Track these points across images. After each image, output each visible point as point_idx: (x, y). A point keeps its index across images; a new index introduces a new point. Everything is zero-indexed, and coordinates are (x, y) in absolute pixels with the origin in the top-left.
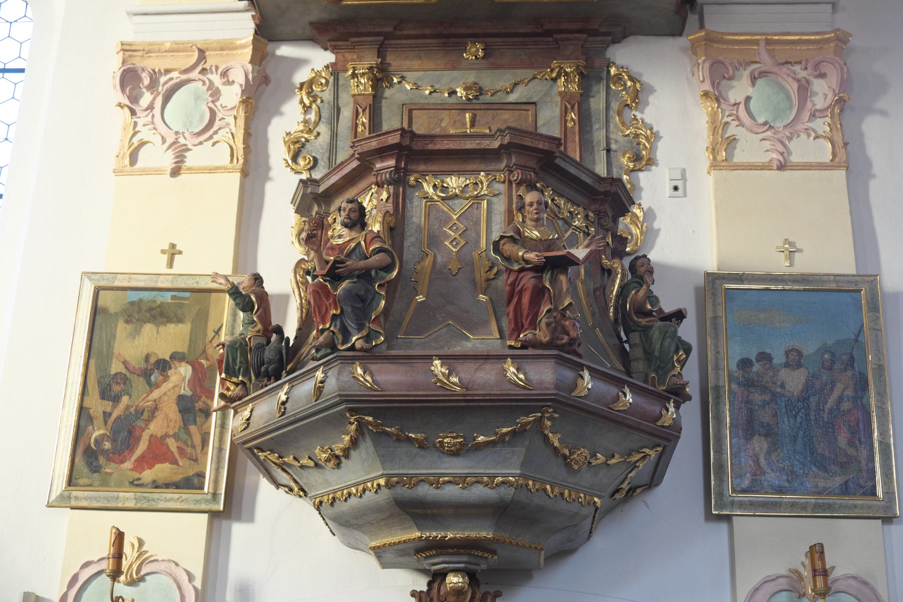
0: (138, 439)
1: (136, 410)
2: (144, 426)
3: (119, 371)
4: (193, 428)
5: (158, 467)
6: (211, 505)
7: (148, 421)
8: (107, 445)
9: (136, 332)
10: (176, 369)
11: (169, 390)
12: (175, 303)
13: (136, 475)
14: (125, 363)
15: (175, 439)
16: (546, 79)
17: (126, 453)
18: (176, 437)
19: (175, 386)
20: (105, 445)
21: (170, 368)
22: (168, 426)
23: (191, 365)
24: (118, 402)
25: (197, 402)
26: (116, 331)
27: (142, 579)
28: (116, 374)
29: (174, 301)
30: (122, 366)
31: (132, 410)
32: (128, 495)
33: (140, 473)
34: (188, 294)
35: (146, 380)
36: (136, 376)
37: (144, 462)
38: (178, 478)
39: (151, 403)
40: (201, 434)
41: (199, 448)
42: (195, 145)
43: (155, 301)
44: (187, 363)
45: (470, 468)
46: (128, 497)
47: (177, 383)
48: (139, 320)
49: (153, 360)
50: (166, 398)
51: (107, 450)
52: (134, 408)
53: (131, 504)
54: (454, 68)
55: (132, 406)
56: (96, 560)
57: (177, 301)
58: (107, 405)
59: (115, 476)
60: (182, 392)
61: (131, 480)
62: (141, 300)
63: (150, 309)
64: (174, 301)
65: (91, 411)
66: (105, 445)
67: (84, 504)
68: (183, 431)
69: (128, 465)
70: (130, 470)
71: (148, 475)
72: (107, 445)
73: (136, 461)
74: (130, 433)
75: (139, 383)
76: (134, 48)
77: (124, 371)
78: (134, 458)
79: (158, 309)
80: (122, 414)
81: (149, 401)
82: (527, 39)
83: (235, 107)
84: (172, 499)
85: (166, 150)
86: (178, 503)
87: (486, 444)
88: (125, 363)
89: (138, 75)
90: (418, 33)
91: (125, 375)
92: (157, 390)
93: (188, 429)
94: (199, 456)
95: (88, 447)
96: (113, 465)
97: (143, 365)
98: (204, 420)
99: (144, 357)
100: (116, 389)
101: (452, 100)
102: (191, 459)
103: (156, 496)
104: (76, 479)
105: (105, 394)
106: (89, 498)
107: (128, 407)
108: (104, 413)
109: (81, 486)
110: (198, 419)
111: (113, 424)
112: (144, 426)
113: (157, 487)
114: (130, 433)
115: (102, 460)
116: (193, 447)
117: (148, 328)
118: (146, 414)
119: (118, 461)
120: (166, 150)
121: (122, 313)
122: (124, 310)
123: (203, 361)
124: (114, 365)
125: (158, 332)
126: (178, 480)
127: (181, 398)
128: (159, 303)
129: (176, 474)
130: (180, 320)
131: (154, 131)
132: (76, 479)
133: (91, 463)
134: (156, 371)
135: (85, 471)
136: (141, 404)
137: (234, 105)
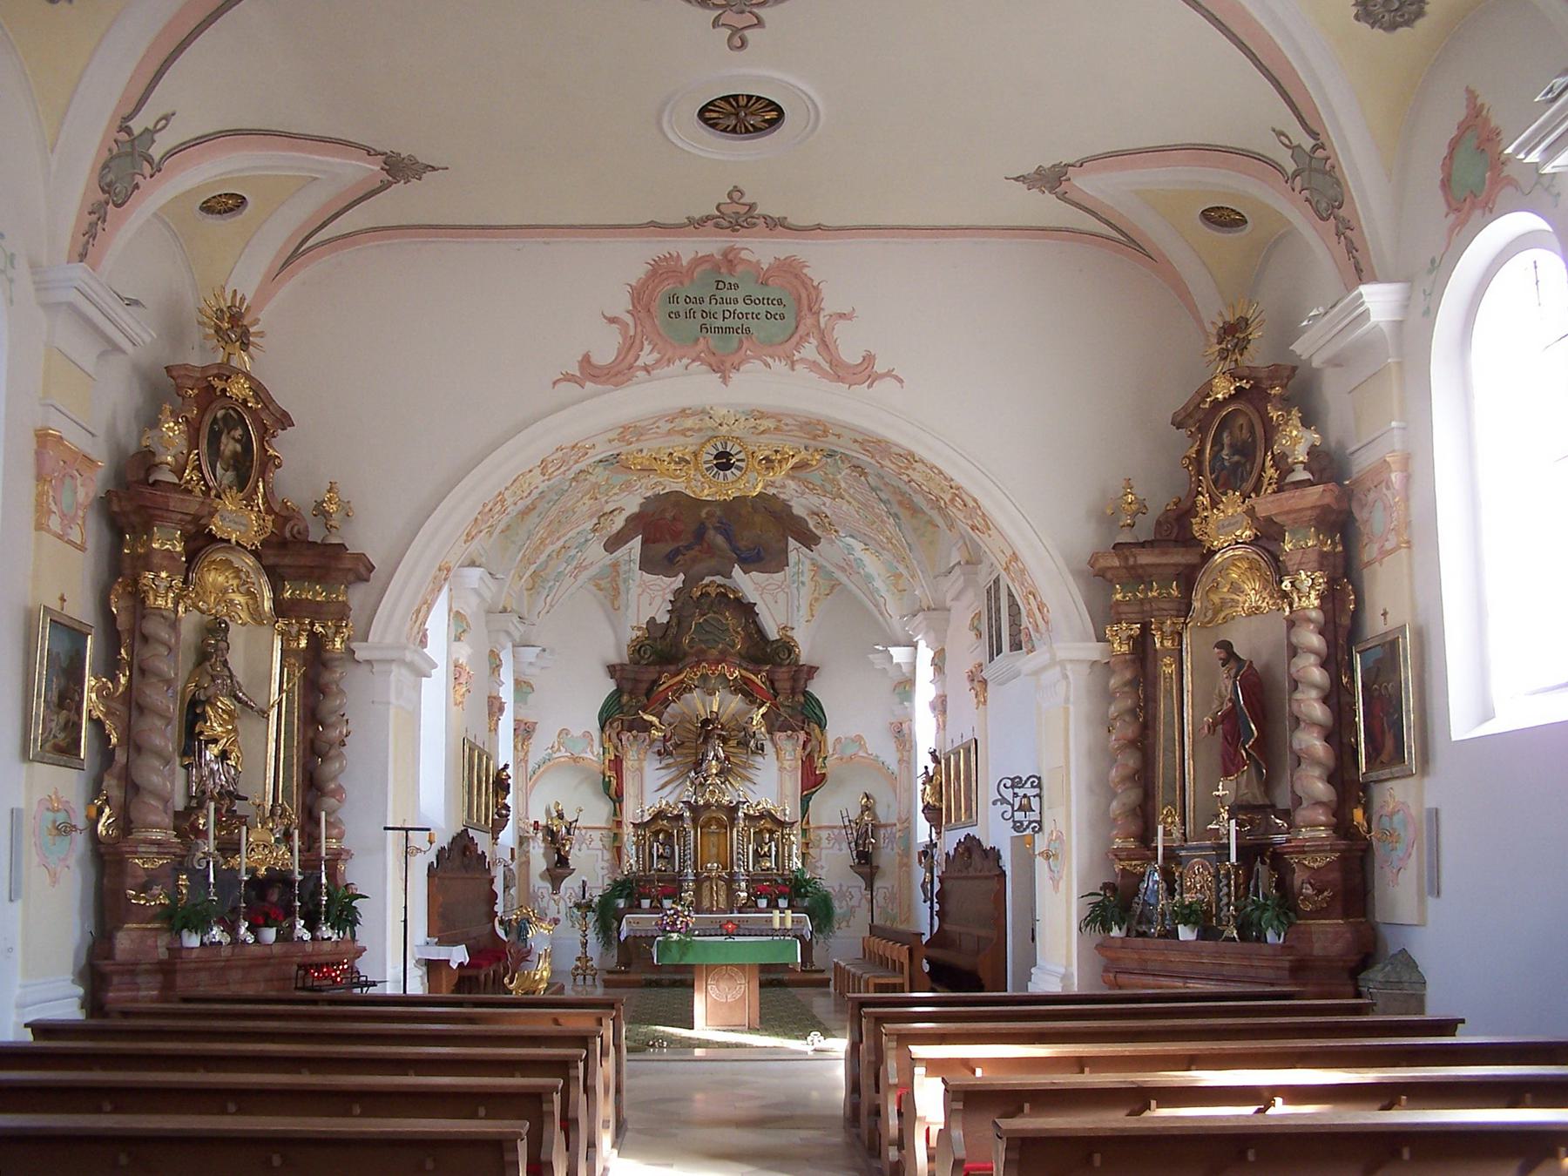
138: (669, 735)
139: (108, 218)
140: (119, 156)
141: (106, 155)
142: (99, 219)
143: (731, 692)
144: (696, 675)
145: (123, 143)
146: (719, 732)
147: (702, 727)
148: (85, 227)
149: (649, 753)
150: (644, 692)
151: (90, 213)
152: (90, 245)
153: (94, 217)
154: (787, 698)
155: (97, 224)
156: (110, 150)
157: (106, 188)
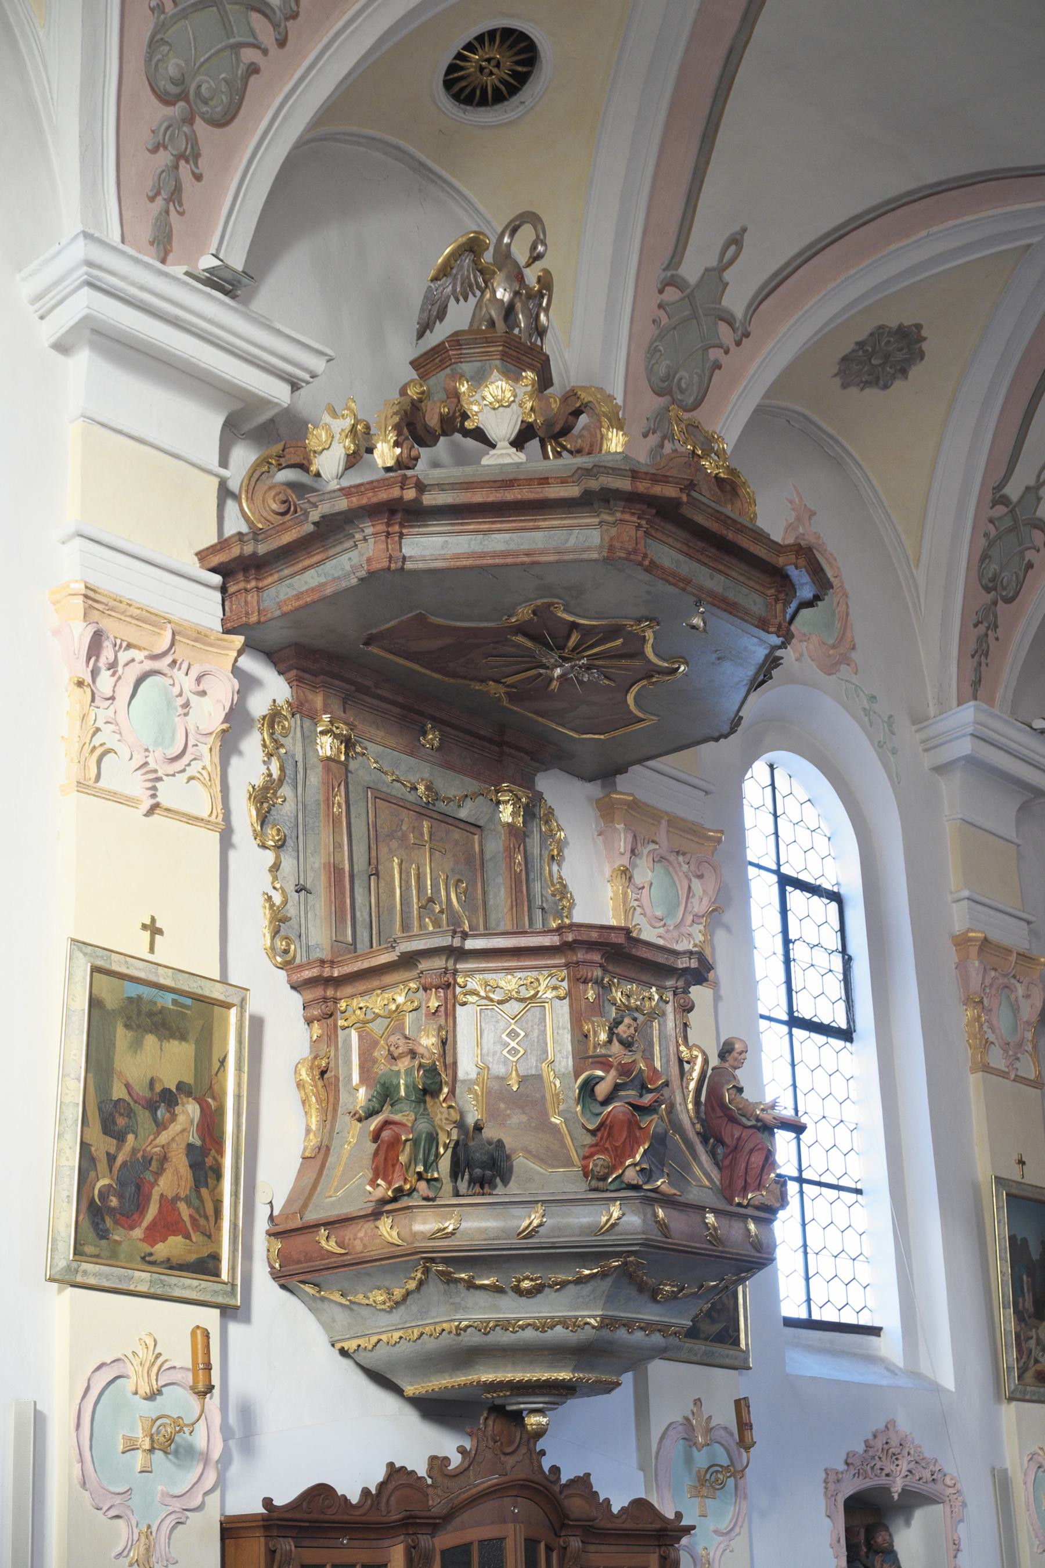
0: (148, 1198)
1: (143, 1156)
2: (153, 1180)
3: (121, 1097)
4: (204, 1191)
5: (172, 1239)
6: (228, 1299)
7: (158, 1173)
8: (114, 1202)
9: (137, 1045)
10: (183, 1106)
11: (178, 1135)
12: (177, 1010)
13: (146, 1248)
14: (127, 1086)
15: (187, 1203)
16: (492, 800)
17: (135, 1217)
18: (187, 1200)
19: (183, 1130)
20: (111, 1201)
21: (177, 1104)
22: (179, 1185)
23: (198, 1103)
24: (123, 1141)
25: (207, 1157)
26: (115, 1037)
27: (160, 1392)
28: (119, 1100)
29: (175, 1008)
30: (124, 1090)
31: (139, 1155)
32: (144, 1275)
33: (152, 1246)
34: (188, 1002)
35: (152, 1115)
36: (140, 1107)
37: (158, 1231)
38: (192, 1258)
39: (159, 1149)
40: (213, 1201)
41: (212, 1220)
42: (167, 775)
43: (155, 1003)
44: (194, 1099)
45: (660, 1315)
46: (142, 1279)
47: (185, 1127)
48: (139, 1026)
49: (158, 1088)
50: (174, 1145)
51: (114, 1209)
52: (141, 1153)
53: (143, 1288)
54: (412, 754)
55: (139, 1151)
56: (109, 1362)
57: (179, 1009)
58: (111, 1144)
59: (124, 1247)
60: (191, 1140)
61: (143, 1255)
62: (139, 998)
63: (151, 1014)
64: (175, 1008)
65: (93, 1149)
66: (111, 1201)
67: (92, 1281)
68: (194, 1194)
69: (138, 1233)
70: (140, 1240)
71: (162, 1250)
72: (114, 1202)
73: (147, 1228)
74: (138, 1187)
75: (143, 1116)
76: (98, 597)
77: (127, 1098)
78: (145, 1223)
79: (160, 1016)
80: (128, 1159)
81: (157, 1147)
82: (477, 741)
83: (211, 734)
84: (189, 1287)
85: (136, 770)
86: (195, 1293)
87: (592, 1276)
88: (127, 1086)
89: (101, 640)
90: (391, 697)
91: (129, 1104)
92: (164, 1132)
93: (199, 1191)
94: (213, 1231)
95: (92, 1202)
96: (121, 1230)
97: (147, 1094)
98: (216, 1182)
99: (148, 1082)
100: (121, 1121)
101: (411, 797)
102: (204, 1234)
103: (173, 1280)
104: (81, 1245)
105: (108, 1127)
106: (100, 1274)
107: (134, 1151)
108: (108, 1154)
109: (87, 1256)
110: (209, 1180)
111: (119, 1171)
112: (153, 1180)
113: (171, 1268)
114: (138, 1187)
115: (109, 1222)
116: (207, 1218)
117: (150, 1040)
118: (154, 1164)
119: (126, 1226)
120: (136, 770)
121: (120, 1012)
122: (122, 1008)
123: (210, 1100)
124: (115, 1087)
125: (161, 1050)
126: (192, 1261)
127: (190, 1147)
128: (159, 1006)
129: (190, 1252)
130: (183, 1038)
131: (118, 737)
132: (81, 1245)
133: (98, 1224)
134: (163, 1104)
135: (90, 1235)
136: (149, 1149)
137: (211, 731)
139: (999, 624)
140: (999, 537)
141: (983, 542)
142: (988, 628)
145: (1000, 518)
148: (972, 645)
151: (976, 626)
152: (984, 666)
153: (982, 628)
155: (986, 635)
156: (986, 535)
157: (990, 585)
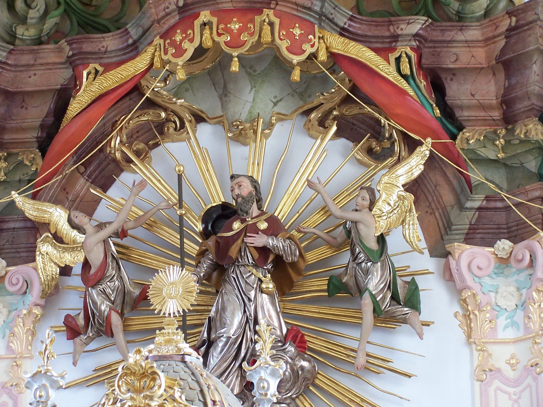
138: (96, 259)
143: (308, 129)
144: (180, 52)
146: (260, 240)
147: (205, 235)
149: (46, 333)
150: (32, 135)
154: (491, 139)
